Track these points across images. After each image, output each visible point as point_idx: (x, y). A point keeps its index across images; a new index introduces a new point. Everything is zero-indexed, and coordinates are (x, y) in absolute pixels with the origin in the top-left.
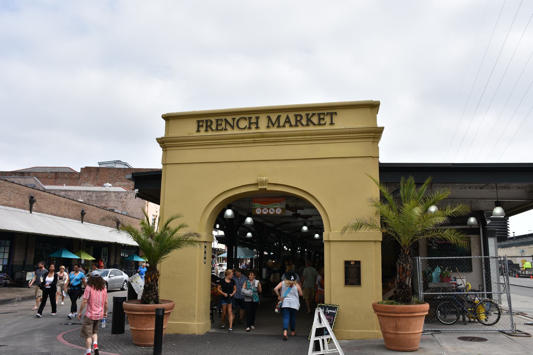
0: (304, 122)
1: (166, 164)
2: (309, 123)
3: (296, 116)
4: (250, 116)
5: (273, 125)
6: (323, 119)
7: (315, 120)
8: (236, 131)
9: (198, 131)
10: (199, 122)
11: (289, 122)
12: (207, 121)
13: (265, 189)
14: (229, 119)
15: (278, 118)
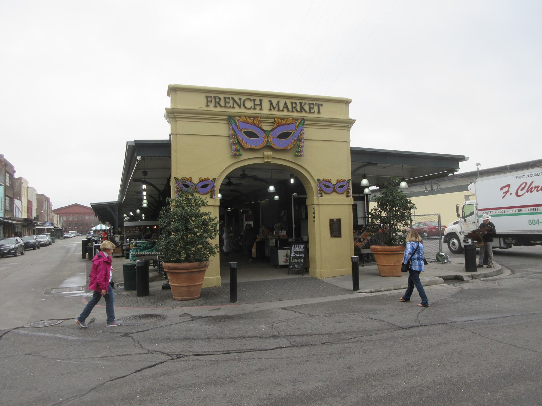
0: (298, 108)
1: (176, 134)
2: (303, 110)
3: (292, 103)
4: (254, 98)
5: (274, 108)
7: (307, 108)
8: (243, 110)
9: (207, 106)
10: (207, 97)
11: (287, 108)
12: (215, 98)
13: (269, 162)
14: (236, 98)
15: (278, 103)
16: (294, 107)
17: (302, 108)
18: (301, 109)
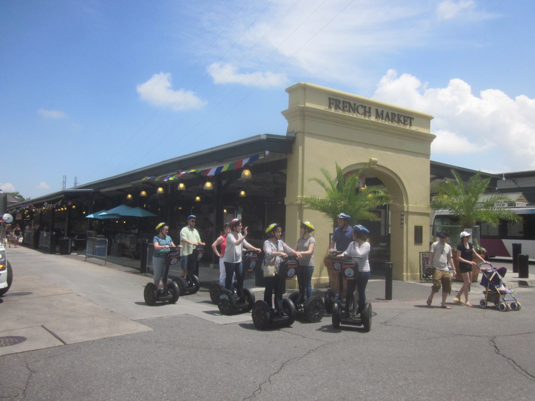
7: (402, 119)
10: (330, 99)
12: (336, 100)
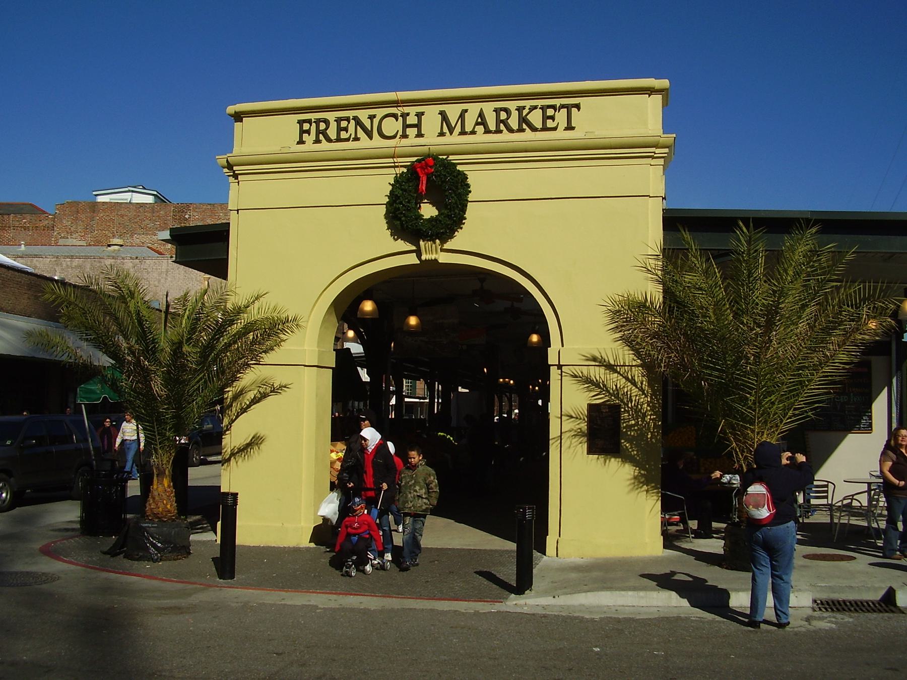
0: (514, 122)
2: (525, 126)
3: (497, 111)
4: (406, 110)
6: (552, 118)
7: (536, 118)
8: (377, 141)
9: (302, 142)
10: (301, 122)
12: (318, 121)
13: (436, 260)
14: (363, 115)
15: (462, 116)
16: (502, 121)
17: (523, 120)
18: (520, 125)
